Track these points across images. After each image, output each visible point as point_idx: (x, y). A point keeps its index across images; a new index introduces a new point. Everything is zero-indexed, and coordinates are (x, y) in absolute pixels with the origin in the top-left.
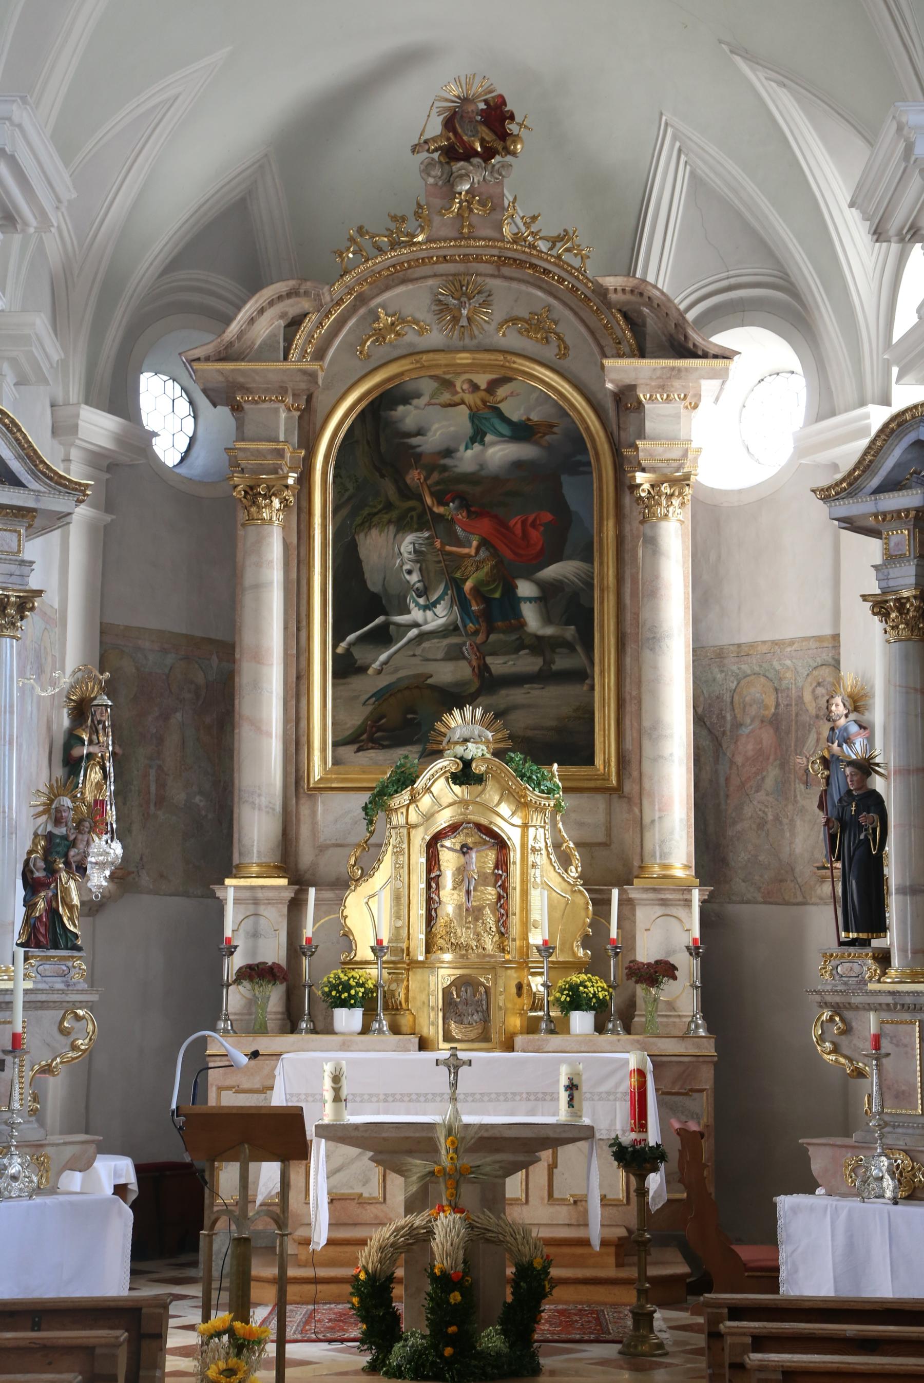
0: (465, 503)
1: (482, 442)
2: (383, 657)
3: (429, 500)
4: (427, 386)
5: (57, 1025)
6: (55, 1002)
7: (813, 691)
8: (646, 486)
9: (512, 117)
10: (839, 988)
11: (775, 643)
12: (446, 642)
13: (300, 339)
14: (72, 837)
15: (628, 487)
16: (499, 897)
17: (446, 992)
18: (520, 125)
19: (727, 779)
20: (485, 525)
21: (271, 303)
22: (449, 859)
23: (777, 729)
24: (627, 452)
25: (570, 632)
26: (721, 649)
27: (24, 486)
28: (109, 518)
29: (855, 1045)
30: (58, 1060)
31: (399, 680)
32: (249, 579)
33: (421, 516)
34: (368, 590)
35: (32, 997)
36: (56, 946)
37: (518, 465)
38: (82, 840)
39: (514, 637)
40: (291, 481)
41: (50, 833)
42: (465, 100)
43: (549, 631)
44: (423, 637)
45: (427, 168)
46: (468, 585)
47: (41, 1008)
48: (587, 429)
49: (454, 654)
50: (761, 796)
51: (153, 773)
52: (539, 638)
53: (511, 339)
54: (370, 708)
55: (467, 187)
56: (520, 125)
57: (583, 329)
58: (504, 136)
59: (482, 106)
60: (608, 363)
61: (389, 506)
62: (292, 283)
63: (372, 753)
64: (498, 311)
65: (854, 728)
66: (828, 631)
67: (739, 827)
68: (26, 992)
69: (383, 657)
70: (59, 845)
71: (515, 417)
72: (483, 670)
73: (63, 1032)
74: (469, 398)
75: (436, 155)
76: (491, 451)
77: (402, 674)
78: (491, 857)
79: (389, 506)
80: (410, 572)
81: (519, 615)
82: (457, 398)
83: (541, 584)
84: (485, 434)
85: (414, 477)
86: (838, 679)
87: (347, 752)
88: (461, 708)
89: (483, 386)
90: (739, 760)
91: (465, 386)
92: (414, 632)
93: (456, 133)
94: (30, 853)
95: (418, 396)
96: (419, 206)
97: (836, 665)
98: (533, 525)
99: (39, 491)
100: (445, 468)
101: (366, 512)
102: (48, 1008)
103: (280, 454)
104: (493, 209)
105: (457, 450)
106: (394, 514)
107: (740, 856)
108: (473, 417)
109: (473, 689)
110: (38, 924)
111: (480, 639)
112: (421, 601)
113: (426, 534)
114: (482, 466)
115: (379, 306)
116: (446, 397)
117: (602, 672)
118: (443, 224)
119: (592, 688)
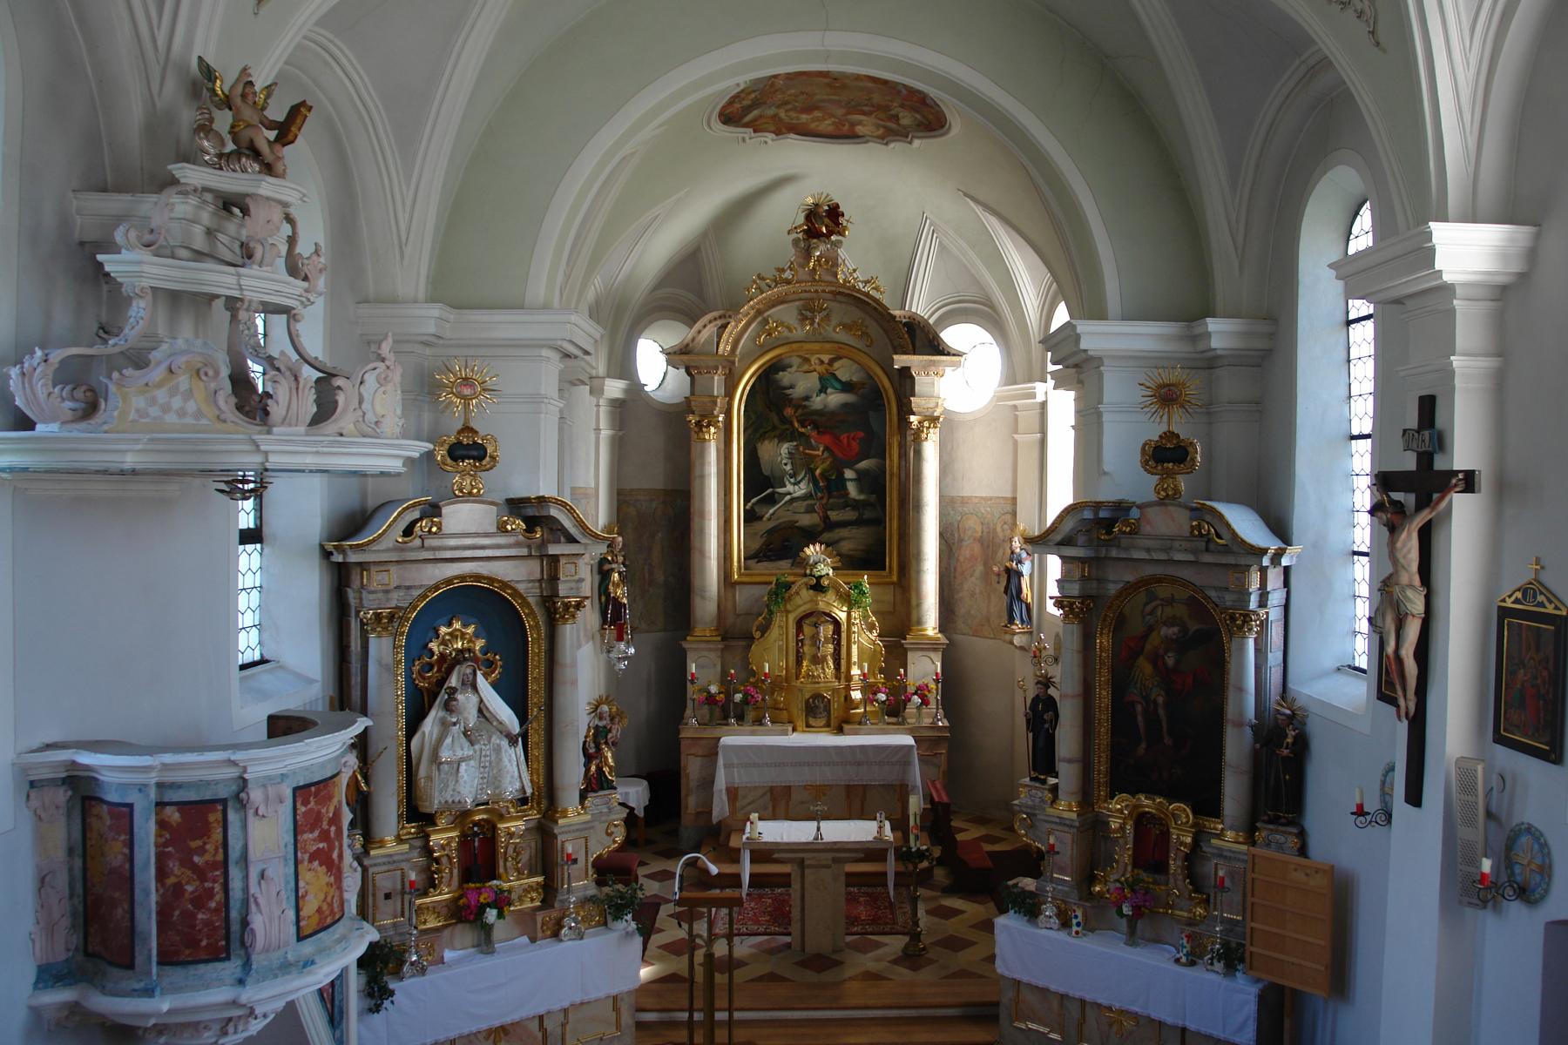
0: (816, 426)
1: (826, 393)
2: (771, 511)
3: (796, 425)
4: (796, 361)
7: (1002, 527)
8: (916, 423)
9: (843, 215)
11: (981, 498)
12: (806, 503)
13: (725, 336)
15: (904, 423)
16: (835, 649)
17: (807, 702)
18: (848, 221)
19: (955, 569)
20: (827, 439)
21: (710, 322)
22: (807, 630)
23: (982, 544)
24: (905, 401)
25: (873, 498)
26: (953, 498)
27: (578, 542)
28: (621, 433)
31: (780, 524)
32: (697, 472)
33: (792, 433)
34: (762, 474)
36: (602, 789)
37: (845, 405)
39: (842, 500)
40: (721, 419)
42: (817, 205)
43: (862, 497)
44: (793, 500)
45: (796, 242)
46: (818, 472)
48: (883, 387)
49: (810, 510)
50: (973, 579)
51: (646, 568)
52: (855, 500)
53: (841, 336)
54: (764, 539)
55: (818, 253)
56: (848, 221)
57: (881, 331)
58: (838, 224)
59: (826, 208)
60: (895, 357)
61: (774, 428)
62: (721, 312)
63: (765, 564)
64: (834, 322)
65: (1024, 555)
66: (1009, 495)
67: (961, 595)
69: (771, 511)
71: (844, 379)
72: (826, 518)
73: (609, 835)
74: (819, 368)
75: (800, 236)
76: (831, 397)
77: (780, 521)
78: (831, 627)
79: (774, 428)
80: (786, 464)
81: (845, 488)
82: (811, 368)
83: (857, 471)
84: (827, 388)
85: (789, 412)
86: (1014, 524)
87: (752, 563)
88: (814, 545)
89: (826, 361)
90: (961, 559)
91: (817, 361)
92: (788, 497)
93: (812, 224)
94: (586, 737)
95: (791, 367)
96: (792, 263)
97: (1014, 514)
98: (853, 439)
100: (805, 407)
101: (762, 431)
103: (715, 404)
104: (832, 266)
105: (811, 397)
106: (777, 433)
107: (961, 610)
108: (821, 379)
109: (820, 529)
111: (824, 501)
112: (792, 480)
113: (795, 443)
114: (825, 406)
115: (769, 316)
116: (806, 367)
117: (890, 520)
118: (803, 274)
119: (885, 528)
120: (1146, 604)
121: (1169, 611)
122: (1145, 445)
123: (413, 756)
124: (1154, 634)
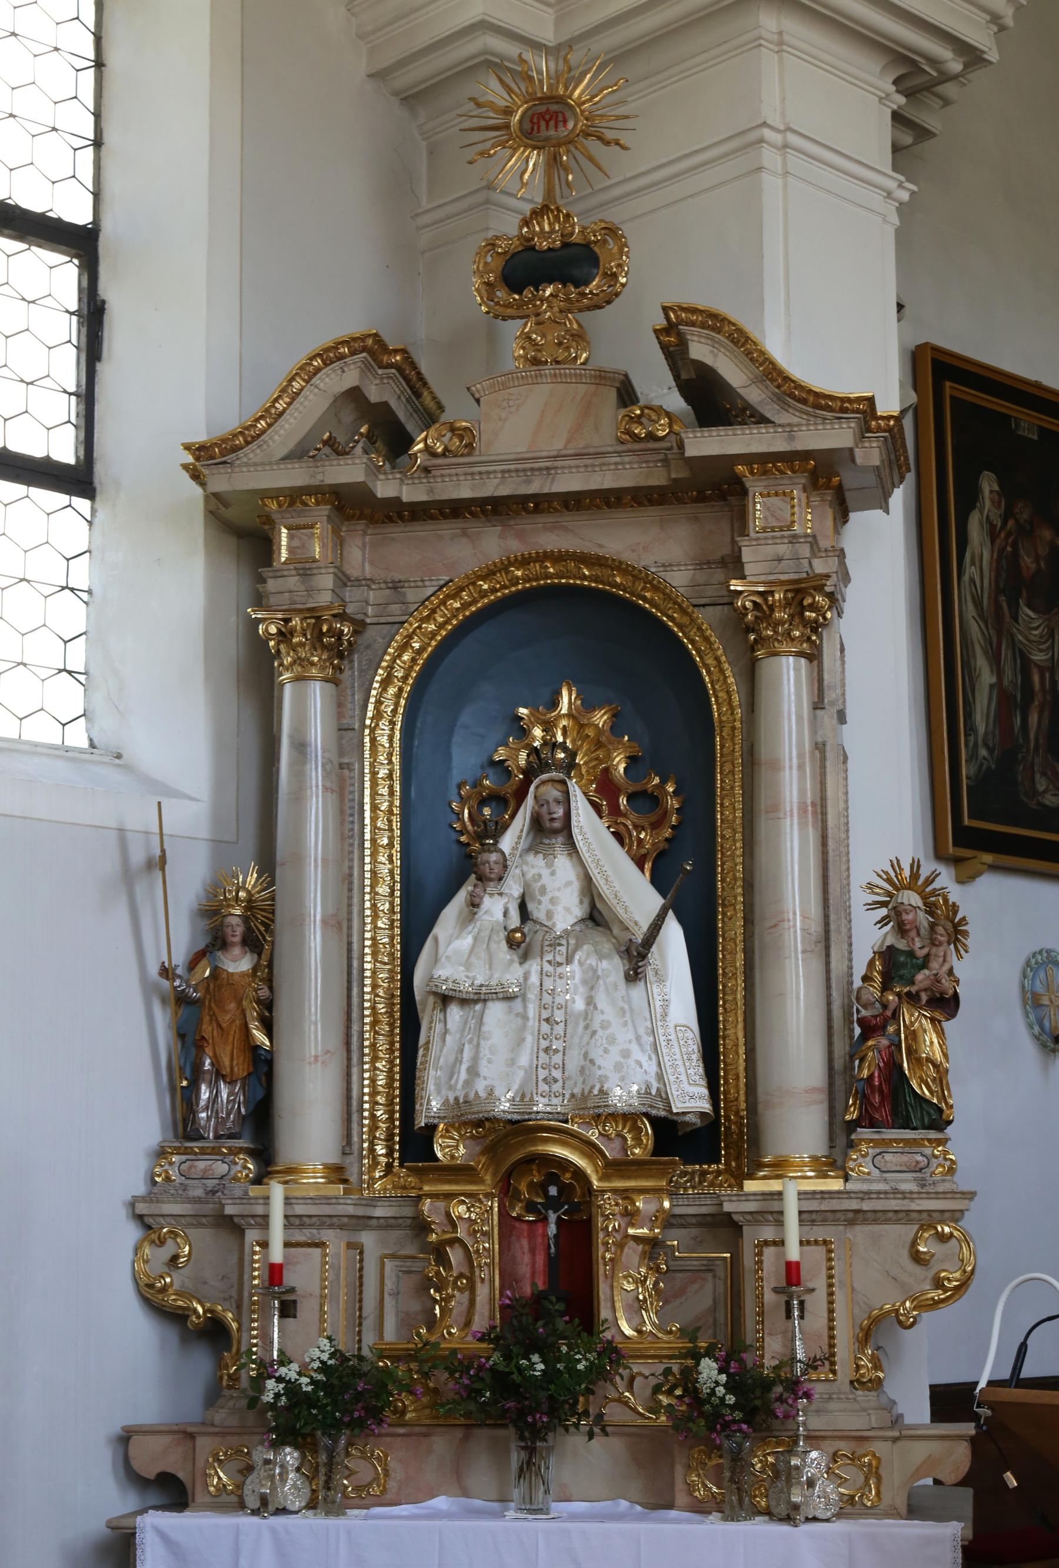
5: (908, 1245)
6: (896, 1212)
14: (921, 953)
30: (908, 1304)
35: (813, 1205)
38: (936, 956)
41: (891, 948)
47: (876, 1221)
68: (802, 1195)
70: (904, 965)
73: (917, 1258)
99: (789, 425)
102: (887, 1221)
110: (868, 1091)
123: (418, 997)
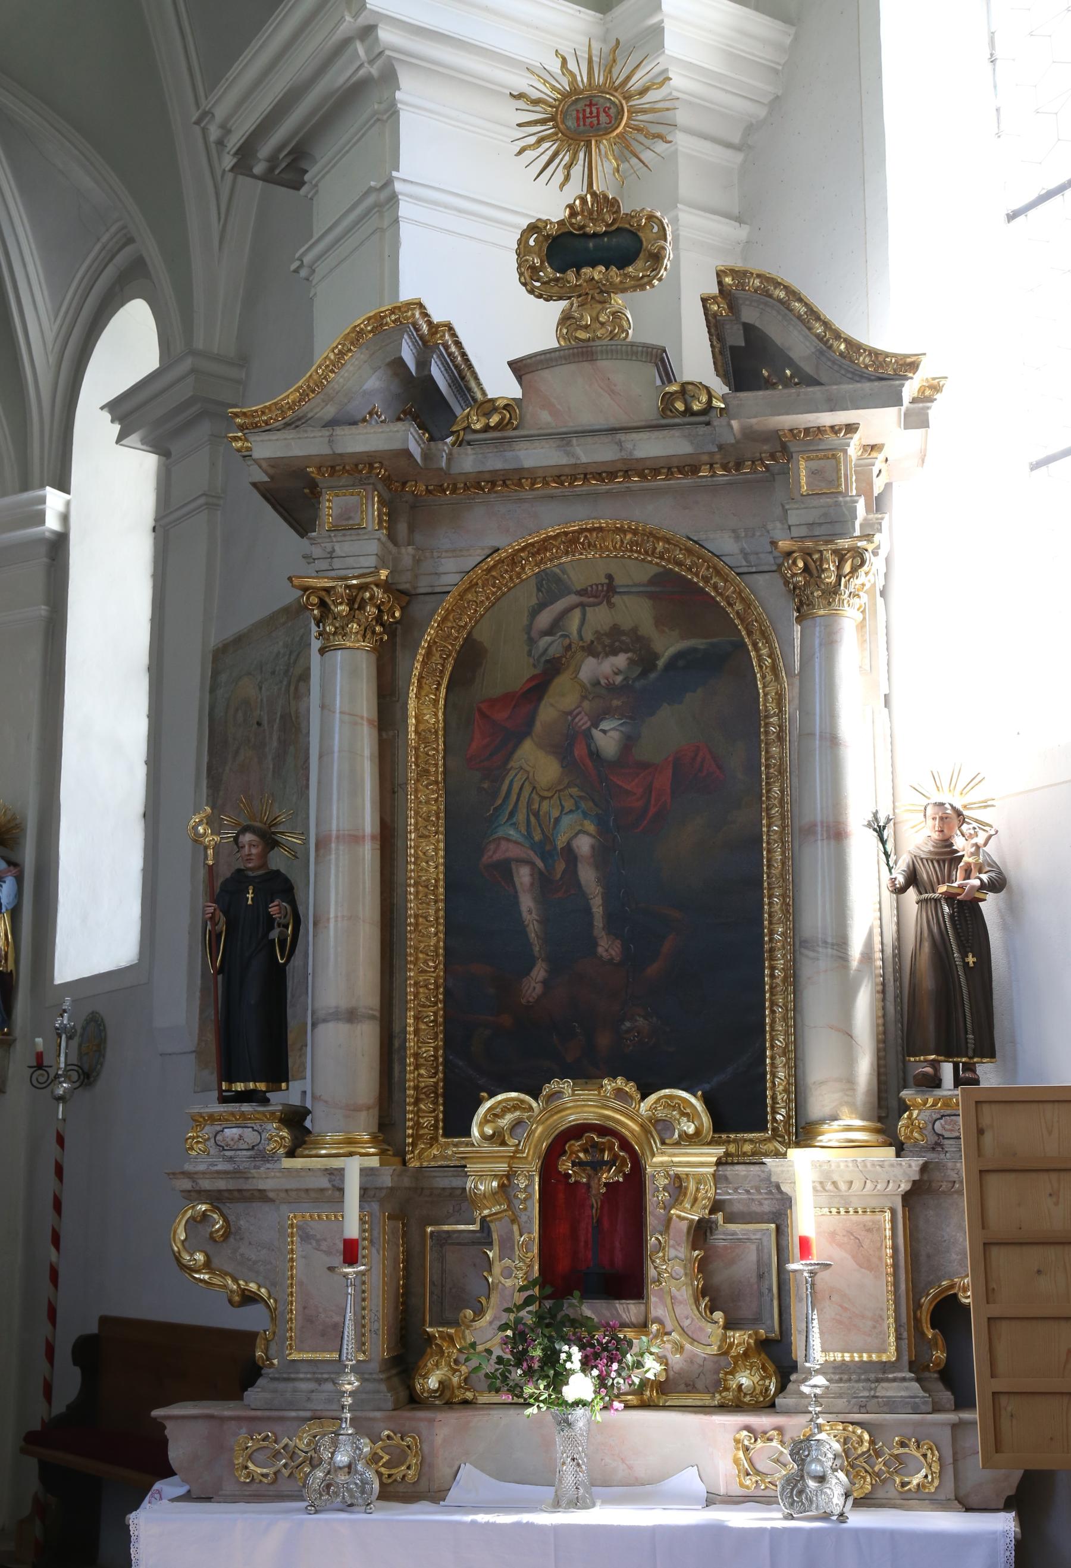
10: (221, 1167)
29: (242, 1255)
120: (535, 612)
121: (600, 618)
122: (533, 228)
124: (562, 681)
